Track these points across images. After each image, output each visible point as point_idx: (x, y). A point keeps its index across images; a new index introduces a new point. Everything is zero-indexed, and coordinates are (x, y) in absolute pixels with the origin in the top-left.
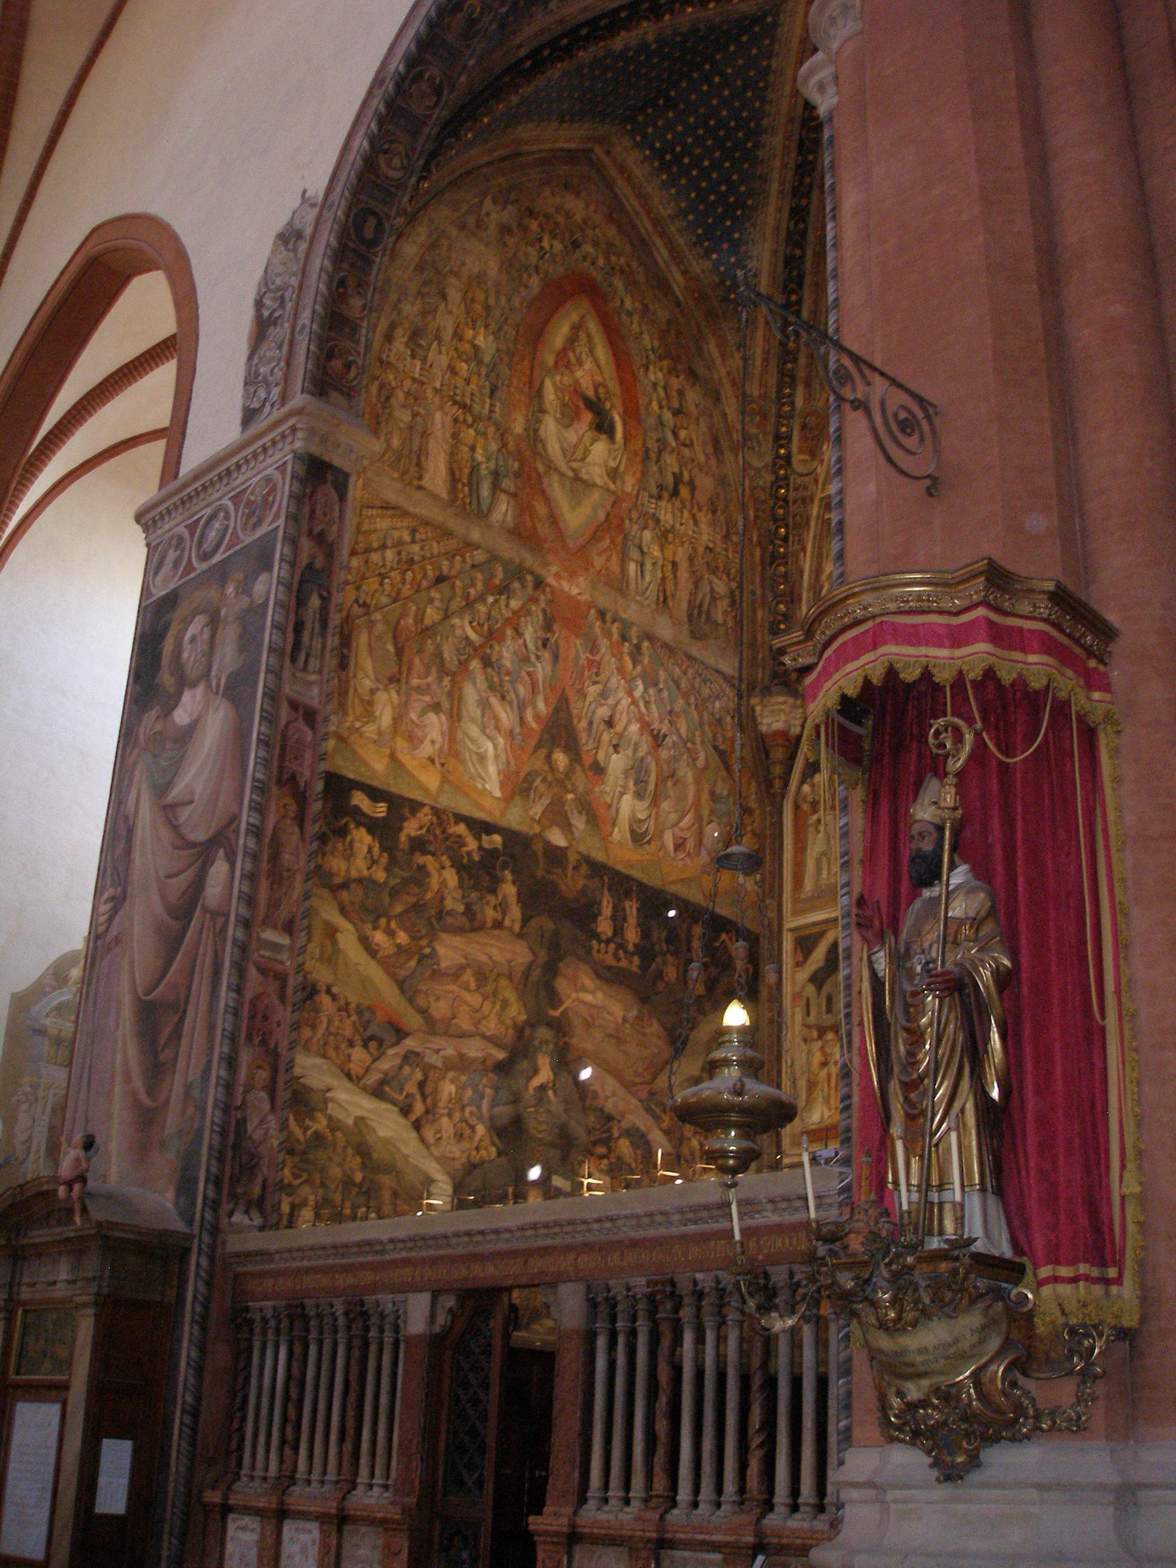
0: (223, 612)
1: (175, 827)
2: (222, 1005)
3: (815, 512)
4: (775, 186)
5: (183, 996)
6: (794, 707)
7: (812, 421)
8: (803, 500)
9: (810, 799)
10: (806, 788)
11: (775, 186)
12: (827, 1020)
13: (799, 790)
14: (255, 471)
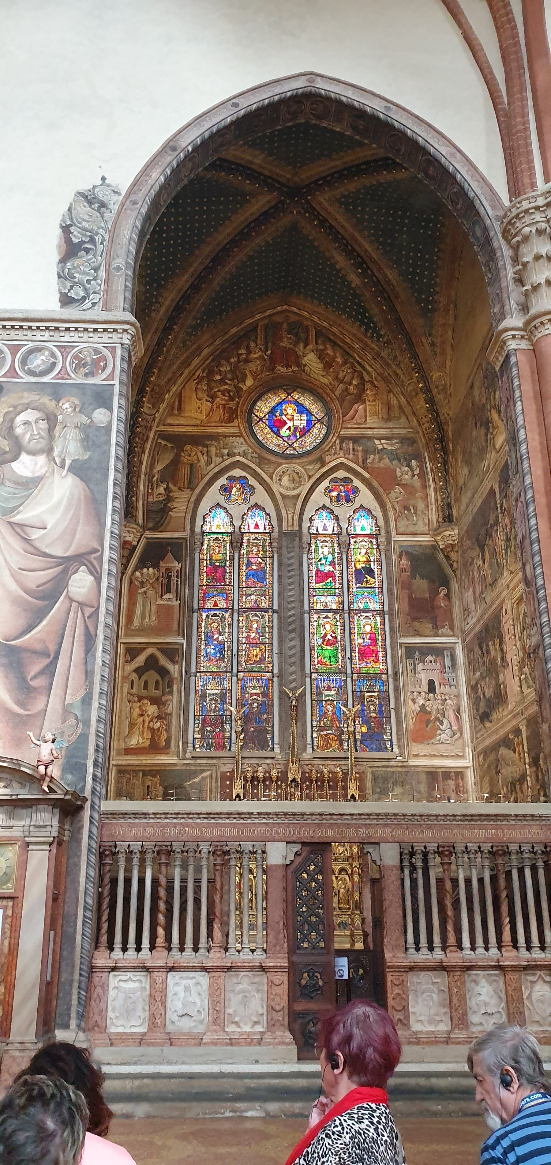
0: (60, 418)
1: (27, 541)
2: (99, 661)
3: (152, 435)
4: (192, 270)
5: (52, 648)
6: (138, 532)
7: (157, 389)
8: (146, 427)
9: (140, 580)
10: (137, 574)
11: (192, 270)
12: (144, 693)
13: (133, 574)
14: (82, 340)
